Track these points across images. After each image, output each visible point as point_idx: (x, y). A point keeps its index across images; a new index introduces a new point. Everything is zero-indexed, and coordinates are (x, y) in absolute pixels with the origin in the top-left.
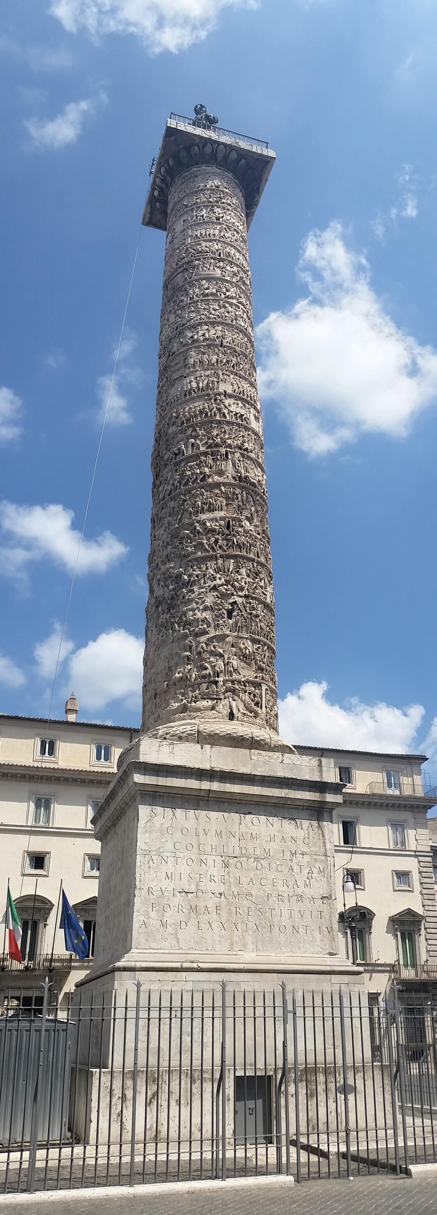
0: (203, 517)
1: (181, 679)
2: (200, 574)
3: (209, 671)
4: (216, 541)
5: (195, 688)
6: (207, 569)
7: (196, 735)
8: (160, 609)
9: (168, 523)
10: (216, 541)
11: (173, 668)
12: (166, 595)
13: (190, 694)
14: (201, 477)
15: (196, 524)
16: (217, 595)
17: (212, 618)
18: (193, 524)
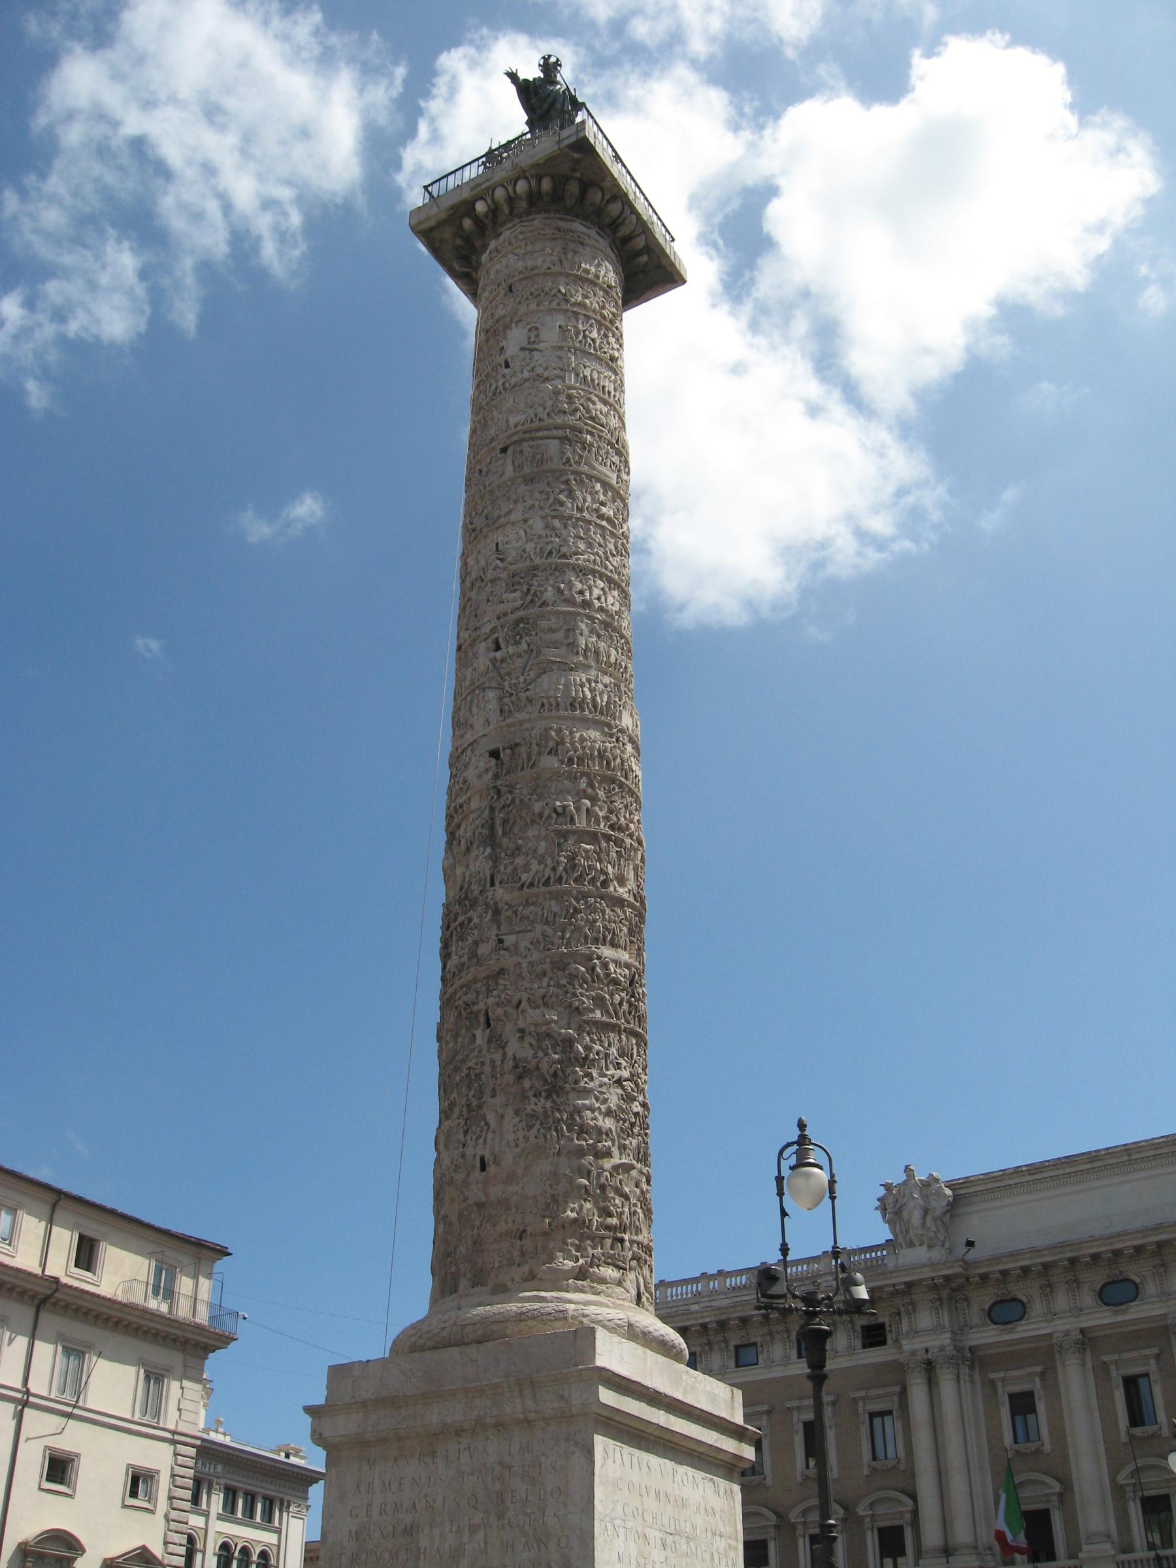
0: (607, 952)
1: (575, 1221)
2: (601, 1051)
3: (614, 1221)
4: (621, 1004)
5: (596, 1243)
6: (610, 1045)
7: (626, 1328)
8: (527, 1083)
9: (542, 935)
10: (621, 1004)
11: (561, 1199)
12: (544, 1066)
13: (590, 1251)
14: (602, 878)
15: (596, 961)
16: (622, 1095)
17: (616, 1131)
18: (589, 958)
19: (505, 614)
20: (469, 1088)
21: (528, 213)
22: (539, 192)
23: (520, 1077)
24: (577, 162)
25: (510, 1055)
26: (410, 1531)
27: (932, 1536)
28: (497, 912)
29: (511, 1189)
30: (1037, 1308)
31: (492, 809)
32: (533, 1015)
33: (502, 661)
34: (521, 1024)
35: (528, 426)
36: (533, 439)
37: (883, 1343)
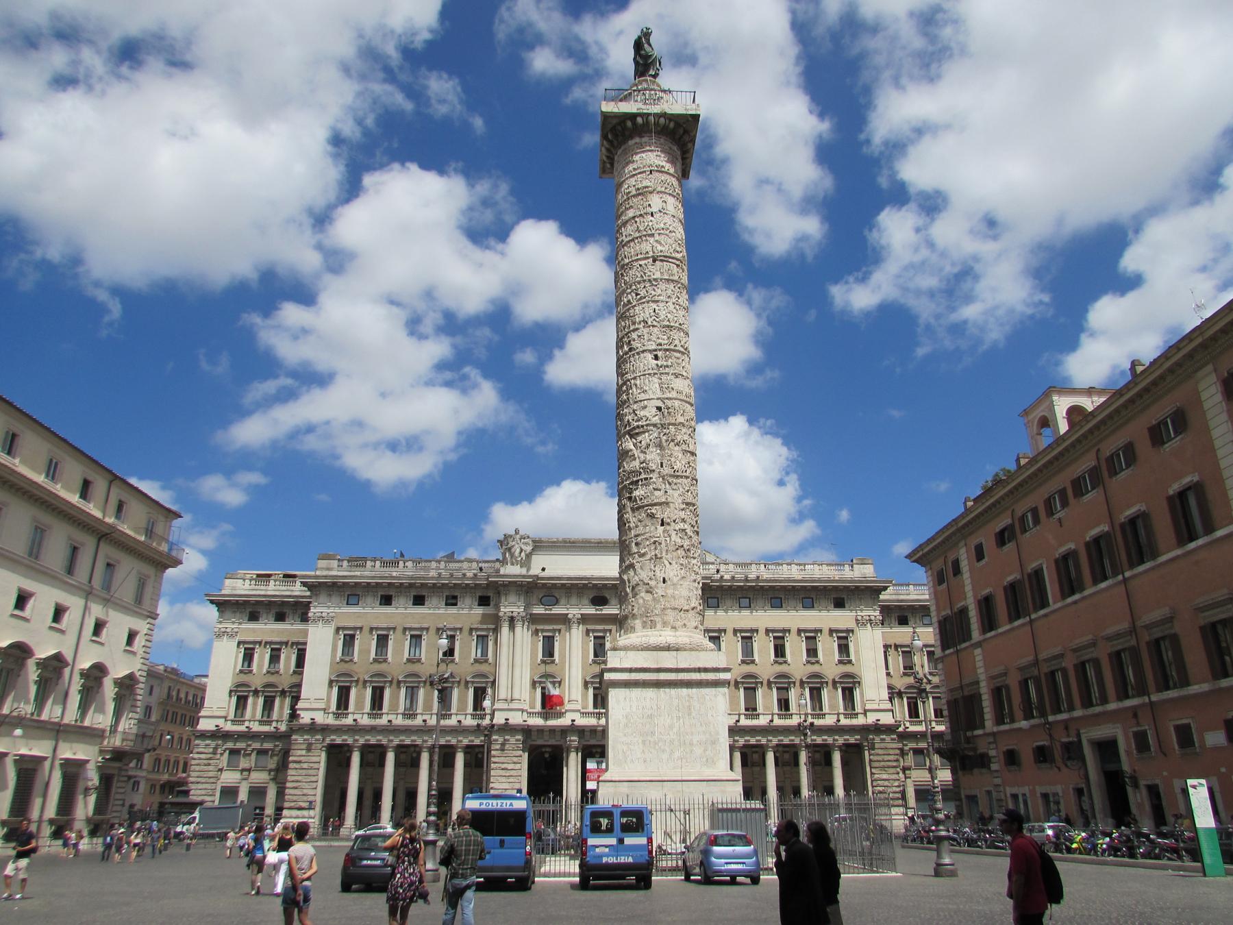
8: (679, 551)
19: (661, 345)
20: (656, 549)
21: (659, 134)
22: (668, 126)
23: (677, 549)
24: (688, 121)
25: (673, 539)
26: (650, 716)
27: (503, 692)
28: (663, 479)
29: (676, 592)
30: (563, 601)
31: (660, 433)
32: (681, 525)
33: (661, 367)
34: (677, 529)
35: (666, 254)
36: (667, 261)
37: (489, 605)
